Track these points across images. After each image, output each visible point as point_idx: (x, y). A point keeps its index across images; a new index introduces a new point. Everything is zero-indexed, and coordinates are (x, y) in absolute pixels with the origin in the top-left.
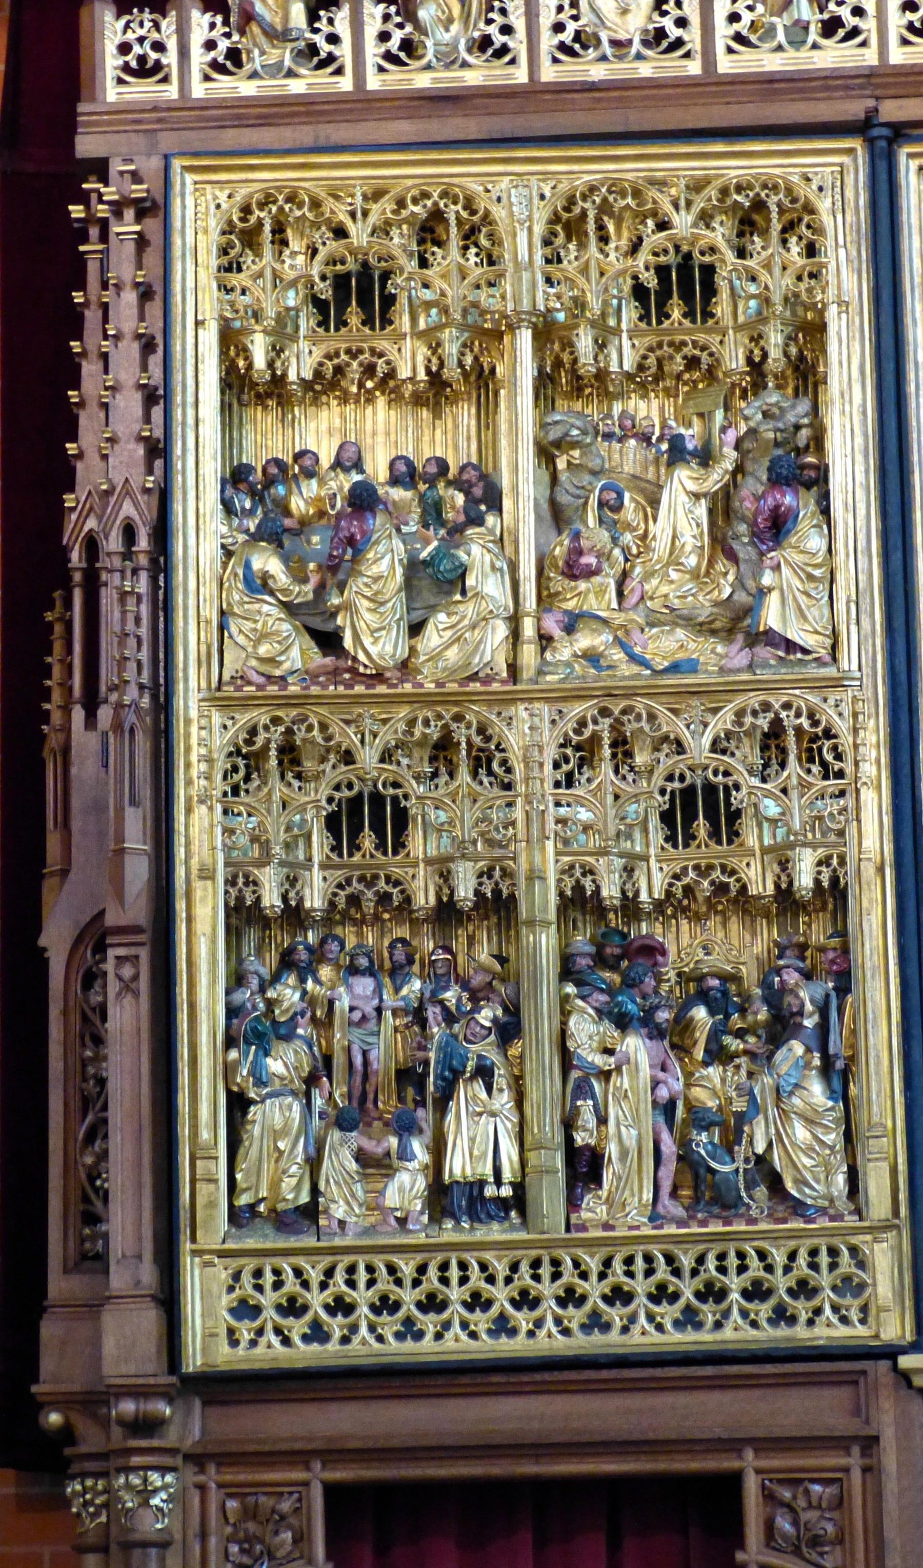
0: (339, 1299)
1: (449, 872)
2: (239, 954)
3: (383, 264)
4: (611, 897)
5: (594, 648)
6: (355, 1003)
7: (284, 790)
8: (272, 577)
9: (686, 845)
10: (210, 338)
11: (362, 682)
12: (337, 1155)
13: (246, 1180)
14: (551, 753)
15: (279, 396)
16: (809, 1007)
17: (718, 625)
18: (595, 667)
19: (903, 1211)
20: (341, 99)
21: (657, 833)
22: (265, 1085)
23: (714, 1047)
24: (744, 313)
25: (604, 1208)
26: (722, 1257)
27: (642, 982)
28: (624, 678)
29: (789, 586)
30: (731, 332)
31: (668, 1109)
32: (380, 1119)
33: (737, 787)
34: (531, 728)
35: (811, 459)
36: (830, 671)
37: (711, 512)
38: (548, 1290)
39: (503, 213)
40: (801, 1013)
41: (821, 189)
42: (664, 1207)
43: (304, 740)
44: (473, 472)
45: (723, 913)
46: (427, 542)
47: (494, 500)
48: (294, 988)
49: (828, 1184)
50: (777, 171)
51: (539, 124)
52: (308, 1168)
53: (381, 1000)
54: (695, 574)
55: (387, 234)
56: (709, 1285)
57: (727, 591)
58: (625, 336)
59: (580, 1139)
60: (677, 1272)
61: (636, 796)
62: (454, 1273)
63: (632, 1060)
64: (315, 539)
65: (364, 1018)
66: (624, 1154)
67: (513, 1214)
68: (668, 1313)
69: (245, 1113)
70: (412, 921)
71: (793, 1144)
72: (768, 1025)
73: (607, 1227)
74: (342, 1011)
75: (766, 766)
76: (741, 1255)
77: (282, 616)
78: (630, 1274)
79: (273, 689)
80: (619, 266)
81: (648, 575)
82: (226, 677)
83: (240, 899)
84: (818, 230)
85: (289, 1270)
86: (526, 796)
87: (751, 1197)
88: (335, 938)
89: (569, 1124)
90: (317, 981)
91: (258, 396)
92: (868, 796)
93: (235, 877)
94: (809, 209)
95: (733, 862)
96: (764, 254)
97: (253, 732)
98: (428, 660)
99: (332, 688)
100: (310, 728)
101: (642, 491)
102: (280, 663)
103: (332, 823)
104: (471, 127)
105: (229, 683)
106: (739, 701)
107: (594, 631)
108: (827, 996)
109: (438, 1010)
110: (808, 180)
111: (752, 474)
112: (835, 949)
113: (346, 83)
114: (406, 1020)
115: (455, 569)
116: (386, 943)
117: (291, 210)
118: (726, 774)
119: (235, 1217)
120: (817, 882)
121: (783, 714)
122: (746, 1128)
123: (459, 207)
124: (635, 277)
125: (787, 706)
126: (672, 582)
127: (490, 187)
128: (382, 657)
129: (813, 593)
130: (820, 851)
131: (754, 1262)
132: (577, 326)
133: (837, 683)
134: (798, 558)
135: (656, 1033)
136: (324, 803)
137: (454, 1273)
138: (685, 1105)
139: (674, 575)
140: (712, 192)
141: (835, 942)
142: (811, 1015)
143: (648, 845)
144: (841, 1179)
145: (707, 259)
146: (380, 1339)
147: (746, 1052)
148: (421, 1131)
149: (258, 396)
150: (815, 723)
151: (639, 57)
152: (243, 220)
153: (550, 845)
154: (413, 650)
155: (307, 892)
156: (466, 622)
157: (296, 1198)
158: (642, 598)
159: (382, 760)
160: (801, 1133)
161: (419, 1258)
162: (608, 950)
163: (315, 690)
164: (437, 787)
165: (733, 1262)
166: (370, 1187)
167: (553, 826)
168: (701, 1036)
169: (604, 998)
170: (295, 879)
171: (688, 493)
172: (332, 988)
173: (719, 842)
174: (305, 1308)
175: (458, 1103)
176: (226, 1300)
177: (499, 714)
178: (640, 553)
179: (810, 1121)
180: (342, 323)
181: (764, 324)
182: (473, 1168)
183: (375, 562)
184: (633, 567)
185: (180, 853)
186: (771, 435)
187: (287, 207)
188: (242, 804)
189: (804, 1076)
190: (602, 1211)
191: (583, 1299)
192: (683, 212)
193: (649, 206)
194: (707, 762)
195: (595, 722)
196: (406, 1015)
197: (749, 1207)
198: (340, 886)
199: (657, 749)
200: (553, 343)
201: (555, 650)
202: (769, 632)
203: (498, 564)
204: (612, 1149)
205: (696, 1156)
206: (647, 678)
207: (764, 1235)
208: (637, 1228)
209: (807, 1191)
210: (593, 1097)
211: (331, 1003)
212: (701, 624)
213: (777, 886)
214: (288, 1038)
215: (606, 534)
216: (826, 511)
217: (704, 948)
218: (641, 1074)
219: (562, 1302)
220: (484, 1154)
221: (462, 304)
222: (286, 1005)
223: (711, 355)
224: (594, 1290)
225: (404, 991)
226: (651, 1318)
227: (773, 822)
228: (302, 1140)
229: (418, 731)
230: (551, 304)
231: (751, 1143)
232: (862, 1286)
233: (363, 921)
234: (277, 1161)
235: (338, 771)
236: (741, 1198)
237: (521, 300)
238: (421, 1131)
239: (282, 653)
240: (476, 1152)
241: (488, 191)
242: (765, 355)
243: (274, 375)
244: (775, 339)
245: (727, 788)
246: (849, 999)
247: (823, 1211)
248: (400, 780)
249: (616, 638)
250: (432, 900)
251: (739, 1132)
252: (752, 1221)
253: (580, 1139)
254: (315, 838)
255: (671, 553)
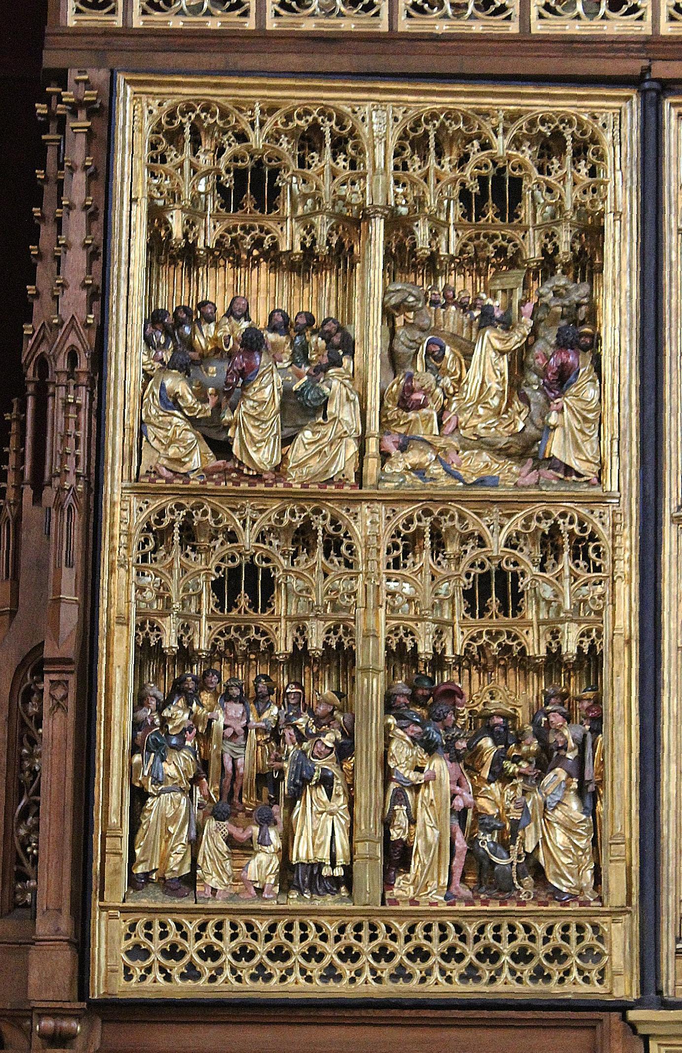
0: (209, 947)
1: (304, 627)
2: (141, 682)
3: (273, 163)
4: (426, 653)
5: (420, 463)
6: (228, 723)
7: (184, 559)
8: (181, 397)
9: (481, 616)
10: (140, 212)
11: (245, 481)
12: (212, 838)
13: (143, 853)
14: (386, 542)
15: (189, 259)
16: (571, 744)
17: (513, 450)
18: (421, 478)
19: (635, 900)
20: (248, 35)
21: (460, 606)
22: (161, 783)
23: (497, 769)
24: (542, 215)
25: (412, 887)
26: (497, 928)
27: (445, 717)
28: (444, 488)
29: (570, 425)
30: (531, 229)
31: (461, 815)
32: (243, 811)
33: (523, 574)
34: (371, 522)
35: (587, 329)
36: (597, 491)
37: (509, 363)
38: (366, 947)
39: (366, 130)
40: (565, 748)
41: (604, 125)
42: (456, 888)
43: (200, 522)
44: (333, 325)
45: (505, 667)
46: (300, 377)
47: (349, 347)
48: (184, 711)
49: (579, 877)
50: (571, 110)
51: (396, 64)
52: (190, 847)
53: (248, 721)
54: (497, 413)
55: (277, 140)
56: (487, 949)
57: (520, 426)
58: (452, 228)
59: (395, 834)
60: (463, 939)
61: (448, 577)
62: (297, 932)
63: (437, 777)
64: (212, 369)
65: (235, 735)
66: (428, 847)
67: (343, 889)
68: (456, 969)
69: (144, 803)
70: (271, 661)
71: (555, 846)
72: (537, 755)
73: (413, 902)
74: (219, 728)
75: (544, 559)
76: (512, 928)
77: (188, 427)
78: (428, 938)
79: (178, 482)
80: (452, 175)
81: (461, 410)
82: (143, 471)
83: (147, 641)
84: (602, 157)
85: (173, 924)
86: (366, 574)
87: (520, 884)
88: (215, 672)
89: (387, 823)
90: (200, 704)
91: (172, 257)
92: (621, 587)
93: (144, 623)
94: (595, 141)
95: (516, 630)
96: (560, 173)
97: (161, 514)
98: (296, 466)
99: (223, 484)
100: (205, 513)
101: (459, 347)
102: (185, 463)
103: (217, 587)
104: (345, 63)
105: (145, 476)
106: (528, 510)
107: (422, 450)
108: (585, 736)
109: (292, 731)
110: (595, 118)
111: (544, 338)
112: (589, 700)
113: (250, 24)
114: (265, 737)
115: (321, 398)
116: (252, 678)
117: (206, 118)
118: (515, 564)
119: (136, 883)
120: (580, 649)
121: (561, 521)
122: (520, 833)
123: (333, 123)
124: (463, 184)
125: (563, 515)
126: (479, 416)
127: (357, 109)
128: (261, 463)
129: (587, 432)
130: (583, 626)
131: (521, 934)
132: (417, 219)
133: (601, 500)
134: (579, 405)
135: (456, 757)
136: (213, 571)
137: (297, 932)
138: (473, 812)
139: (481, 411)
140: (523, 122)
141: (589, 694)
142: (573, 750)
143: (453, 614)
144: (589, 874)
145: (517, 173)
146: (239, 979)
147: (520, 774)
148: (276, 823)
149: (172, 257)
150: (584, 530)
151: (472, 17)
152: (169, 123)
153: (382, 611)
154: (284, 457)
155: (197, 637)
156: (326, 440)
157: (180, 870)
158: (457, 427)
159: (257, 541)
160: (560, 838)
161: (271, 920)
162: (420, 692)
163: (210, 485)
164: (298, 562)
165: (505, 932)
166: (236, 863)
167: (385, 597)
168: (488, 759)
169: (418, 729)
170: (188, 627)
171: (495, 350)
172: (211, 710)
173: (506, 615)
174: (183, 953)
175: (305, 803)
176: (125, 945)
177: (348, 510)
178: (455, 393)
179: (569, 830)
180: (239, 206)
181: (557, 226)
182: (314, 853)
183: (260, 390)
184: (450, 404)
185: (104, 604)
186: (559, 309)
187: (203, 115)
188: (152, 569)
189: (565, 795)
190: (410, 892)
191: (392, 955)
192: (500, 137)
193: (476, 131)
194: (502, 554)
195: (420, 520)
196: (266, 733)
197: (520, 892)
198: (221, 634)
199: (463, 543)
200: (398, 230)
201: (392, 463)
202: (552, 458)
203: (352, 397)
204: (418, 843)
205: (481, 851)
206: (460, 488)
207: (530, 914)
208: (436, 904)
209: (564, 882)
210: (407, 804)
211: (210, 721)
212: (500, 449)
213: (548, 650)
214: (179, 748)
215: (433, 378)
216: (598, 368)
217: (491, 693)
218: (444, 788)
219: (376, 957)
220: (323, 843)
221: (332, 197)
222: (177, 722)
223: (515, 246)
224: (401, 949)
225: (265, 716)
226: (443, 972)
227: (549, 603)
228: (187, 826)
229: (287, 519)
230: (399, 201)
231: (523, 844)
232: (600, 955)
233: (235, 660)
234: (166, 841)
235: (225, 547)
236: (514, 884)
237: (377, 197)
238: (276, 823)
239: (186, 456)
240: (317, 841)
241: (354, 112)
242: (556, 249)
243: (187, 242)
244: (565, 238)
245: (514, 574)
246: (600, 738)
247: (574, 897)
248: (271, 556)
249: (437, 457)
250: (290, 649)
251: (514, 833)
252: (522, 903)
253: (395, 834)
254: (204, 596)
255: (480, 395)
